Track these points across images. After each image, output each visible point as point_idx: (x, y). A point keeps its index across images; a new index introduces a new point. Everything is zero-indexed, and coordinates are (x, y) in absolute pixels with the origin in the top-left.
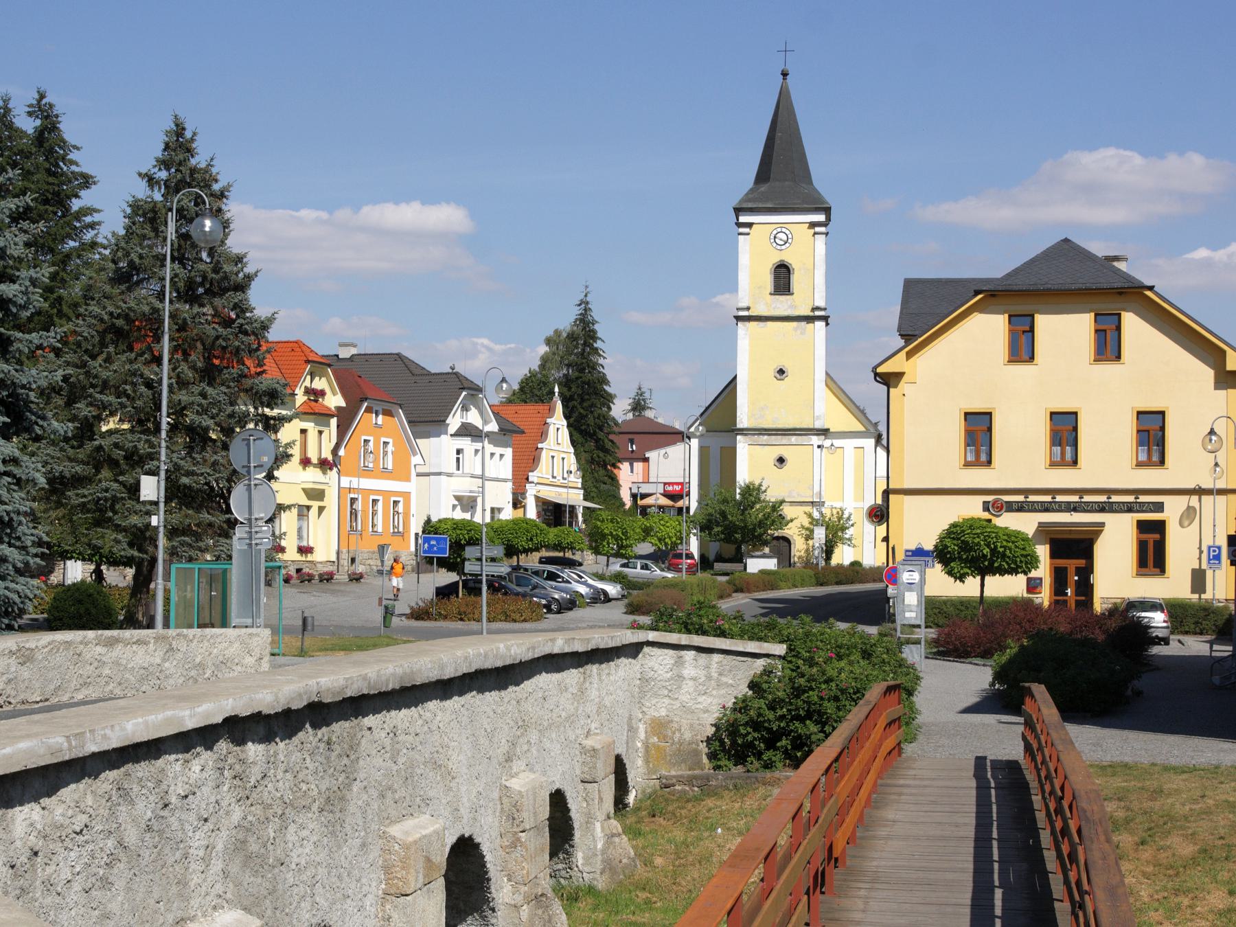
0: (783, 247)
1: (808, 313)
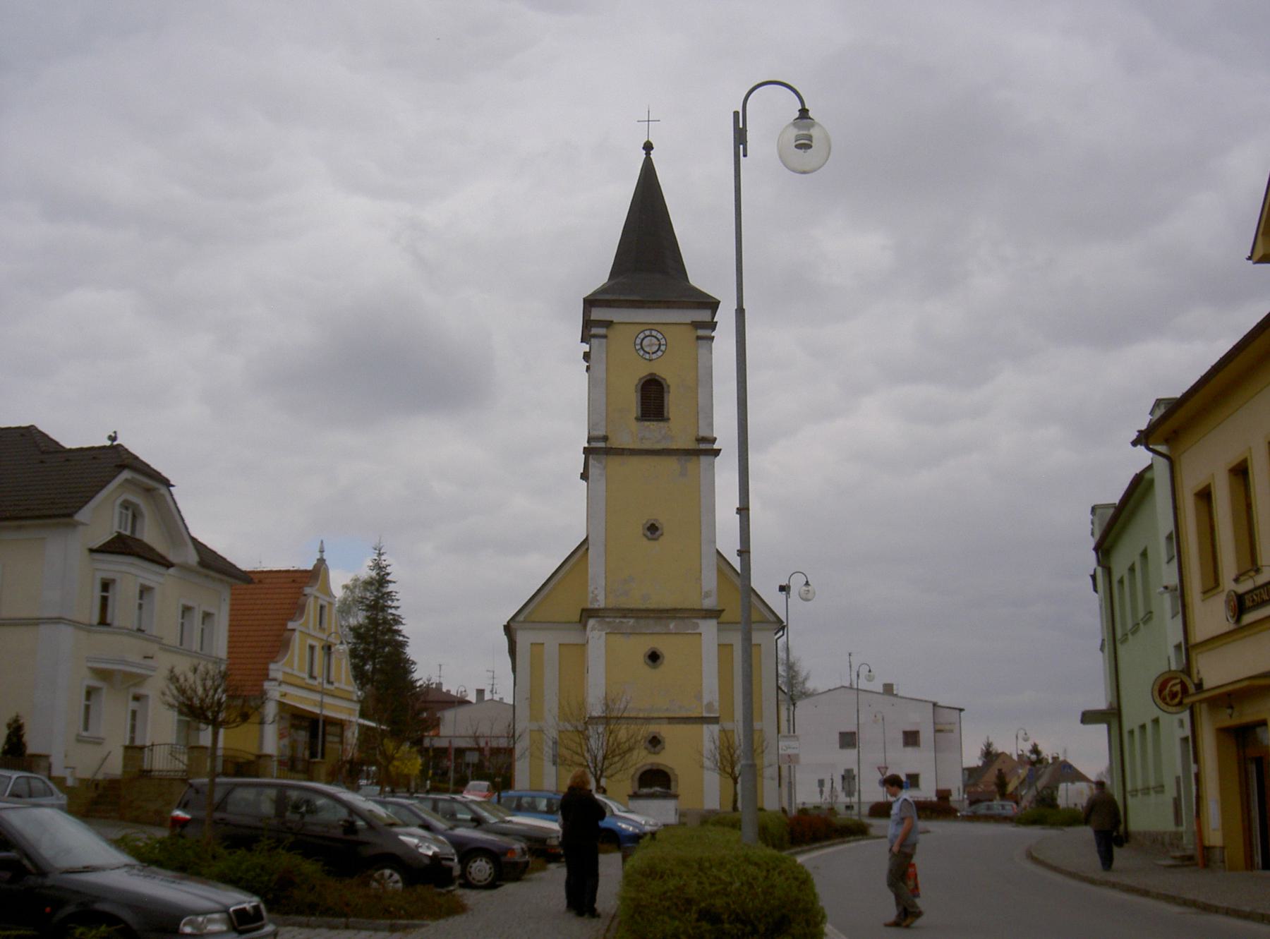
0: (654, 356)
1: (692, 445)
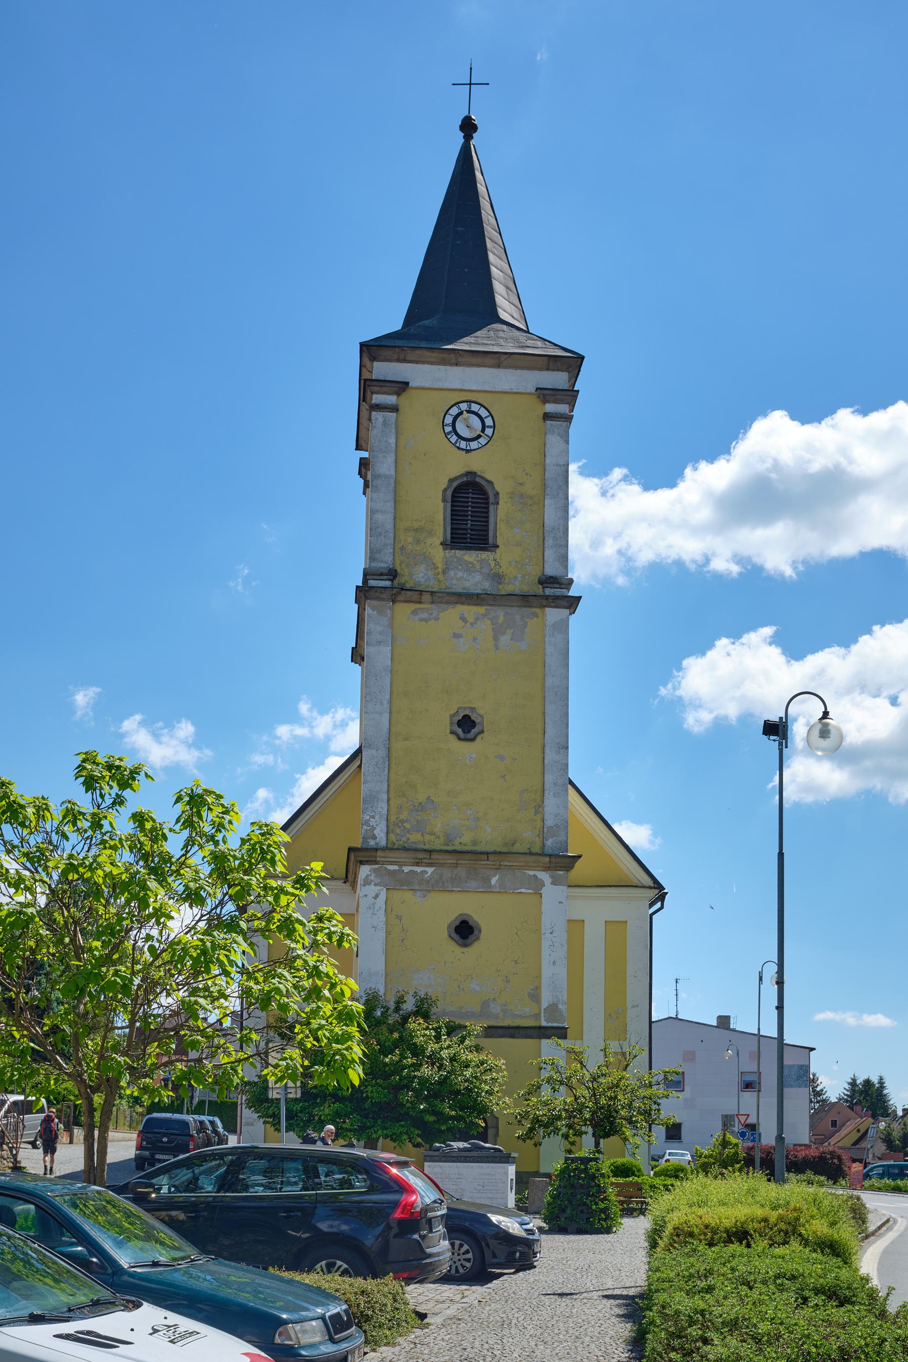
0: (474, 445)
